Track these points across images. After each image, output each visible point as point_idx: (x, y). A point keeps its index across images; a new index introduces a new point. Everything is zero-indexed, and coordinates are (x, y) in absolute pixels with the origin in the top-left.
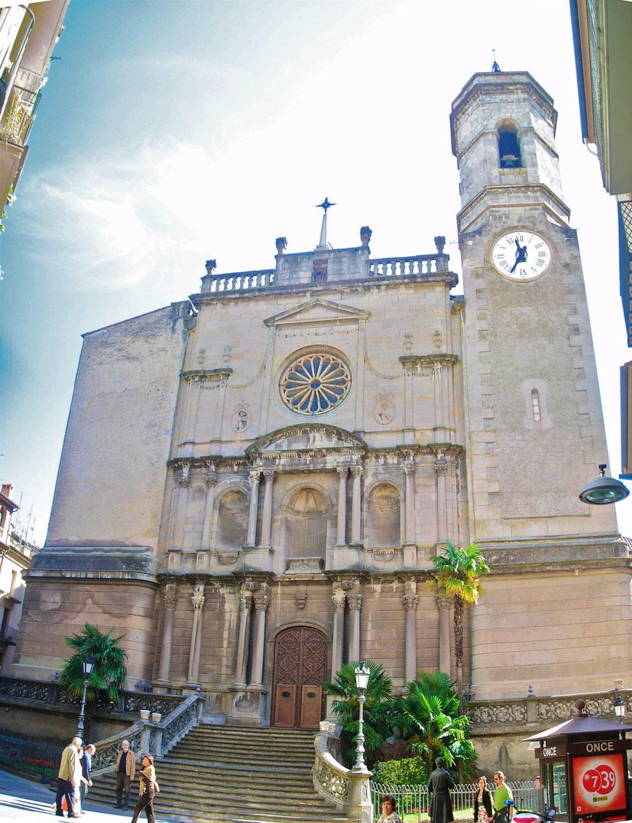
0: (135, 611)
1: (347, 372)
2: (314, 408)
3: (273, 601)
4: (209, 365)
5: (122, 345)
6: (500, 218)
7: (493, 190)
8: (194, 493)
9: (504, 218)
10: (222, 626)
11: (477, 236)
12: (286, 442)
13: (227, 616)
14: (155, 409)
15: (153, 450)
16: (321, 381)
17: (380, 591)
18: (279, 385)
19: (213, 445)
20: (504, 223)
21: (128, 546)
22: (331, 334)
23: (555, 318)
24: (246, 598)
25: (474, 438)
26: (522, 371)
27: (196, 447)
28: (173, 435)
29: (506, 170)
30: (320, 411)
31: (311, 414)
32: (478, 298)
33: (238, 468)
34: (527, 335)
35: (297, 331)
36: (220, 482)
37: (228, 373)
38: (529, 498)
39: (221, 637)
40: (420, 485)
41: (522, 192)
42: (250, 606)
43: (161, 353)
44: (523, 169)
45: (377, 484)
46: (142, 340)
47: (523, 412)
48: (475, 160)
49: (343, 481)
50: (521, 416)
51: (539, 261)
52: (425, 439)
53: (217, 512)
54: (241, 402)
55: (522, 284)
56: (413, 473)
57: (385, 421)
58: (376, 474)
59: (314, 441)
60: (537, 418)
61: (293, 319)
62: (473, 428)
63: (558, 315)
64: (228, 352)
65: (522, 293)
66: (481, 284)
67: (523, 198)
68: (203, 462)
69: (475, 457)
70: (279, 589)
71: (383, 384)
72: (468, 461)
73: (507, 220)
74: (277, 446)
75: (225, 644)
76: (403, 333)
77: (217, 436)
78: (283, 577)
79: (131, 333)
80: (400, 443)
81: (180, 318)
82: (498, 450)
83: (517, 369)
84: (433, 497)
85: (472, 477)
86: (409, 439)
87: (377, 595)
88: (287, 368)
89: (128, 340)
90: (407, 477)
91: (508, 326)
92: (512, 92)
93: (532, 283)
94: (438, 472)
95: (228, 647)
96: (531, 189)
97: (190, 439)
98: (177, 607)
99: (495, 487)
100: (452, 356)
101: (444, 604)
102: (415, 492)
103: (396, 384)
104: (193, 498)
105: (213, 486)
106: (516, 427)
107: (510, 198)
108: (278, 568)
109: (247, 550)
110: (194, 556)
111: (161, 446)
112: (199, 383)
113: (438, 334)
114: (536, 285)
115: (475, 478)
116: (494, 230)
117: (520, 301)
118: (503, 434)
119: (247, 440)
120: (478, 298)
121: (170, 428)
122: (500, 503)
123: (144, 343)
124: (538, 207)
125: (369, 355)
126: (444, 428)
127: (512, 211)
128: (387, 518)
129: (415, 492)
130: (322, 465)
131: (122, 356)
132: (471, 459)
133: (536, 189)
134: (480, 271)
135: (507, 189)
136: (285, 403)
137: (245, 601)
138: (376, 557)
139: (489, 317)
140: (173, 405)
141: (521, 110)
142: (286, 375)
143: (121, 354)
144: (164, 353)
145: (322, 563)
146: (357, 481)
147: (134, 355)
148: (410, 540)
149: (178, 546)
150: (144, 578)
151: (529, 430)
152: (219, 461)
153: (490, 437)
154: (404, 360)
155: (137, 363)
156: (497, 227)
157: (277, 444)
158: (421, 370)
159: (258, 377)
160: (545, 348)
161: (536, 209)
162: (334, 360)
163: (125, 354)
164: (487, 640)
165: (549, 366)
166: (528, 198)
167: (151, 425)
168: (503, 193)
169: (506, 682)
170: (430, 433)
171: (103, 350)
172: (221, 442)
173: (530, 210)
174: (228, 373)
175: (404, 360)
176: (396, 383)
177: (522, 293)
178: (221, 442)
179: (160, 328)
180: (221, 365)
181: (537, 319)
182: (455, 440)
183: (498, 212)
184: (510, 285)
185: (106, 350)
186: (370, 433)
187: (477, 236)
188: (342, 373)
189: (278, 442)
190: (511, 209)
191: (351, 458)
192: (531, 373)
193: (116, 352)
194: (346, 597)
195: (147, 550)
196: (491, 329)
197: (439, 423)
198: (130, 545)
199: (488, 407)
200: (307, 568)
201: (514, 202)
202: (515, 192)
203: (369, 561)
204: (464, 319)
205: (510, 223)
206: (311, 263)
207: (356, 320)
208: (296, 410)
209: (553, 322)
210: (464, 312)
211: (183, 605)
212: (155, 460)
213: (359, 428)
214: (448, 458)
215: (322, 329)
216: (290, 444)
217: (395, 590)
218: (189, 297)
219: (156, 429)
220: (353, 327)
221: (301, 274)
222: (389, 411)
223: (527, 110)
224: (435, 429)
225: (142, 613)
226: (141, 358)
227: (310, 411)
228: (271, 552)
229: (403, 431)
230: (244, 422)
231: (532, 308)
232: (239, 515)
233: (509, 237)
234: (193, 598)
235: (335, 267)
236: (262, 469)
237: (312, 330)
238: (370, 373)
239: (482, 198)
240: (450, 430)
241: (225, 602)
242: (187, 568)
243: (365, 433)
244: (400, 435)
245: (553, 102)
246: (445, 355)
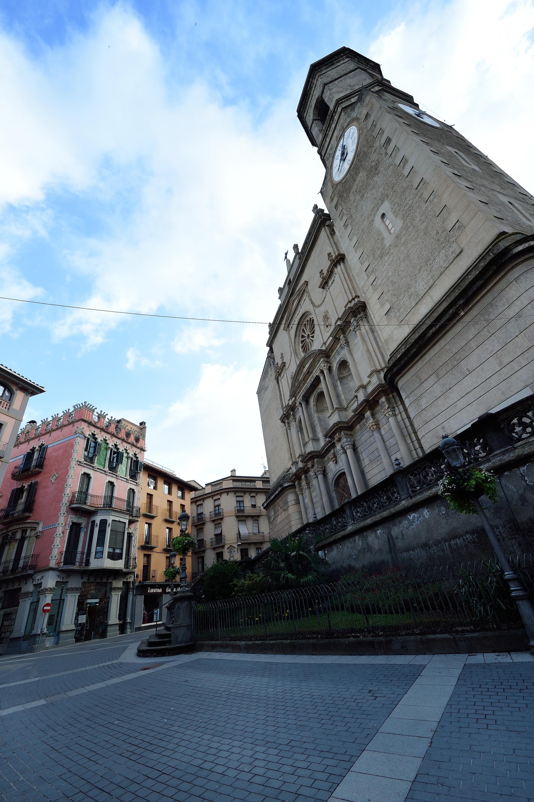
0: (290, 504)
38: (410, 290)
99: (387, 306)
125: (313, 301)
150: (286, 485)
151: (390, 246)
164: (419, 425)
202: (330, 129)
207: (304, 290)
225: (293, 502)
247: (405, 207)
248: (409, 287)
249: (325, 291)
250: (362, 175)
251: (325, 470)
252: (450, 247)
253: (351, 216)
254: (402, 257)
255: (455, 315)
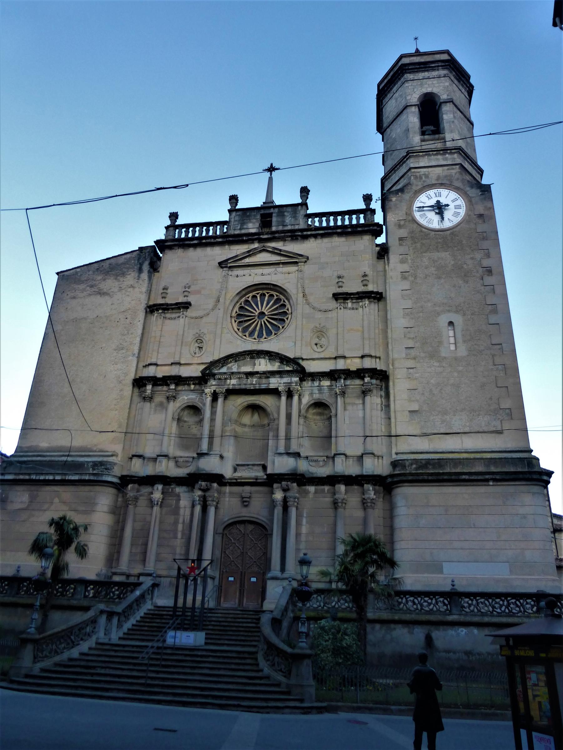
0: (99, 508)
1: (288, 306)
2: (260, 335)
3: (222, 499)
4: (170, 300)
5: (94, 282)
6: (421, 178)
7: (415, 154)
8: (156, 407)
9: (423, 178)
10: (176, 523)
11: (400, 194)
12: (236, 366)
13: (182, 511)
14: (123, 335)
15: (121, 370)
16: (266, 313)
17: (314, 492)
18: (231, 317)
19: (174, 366)
20: (424, 181)
21: (95, 451)
22: (275, 274)
23: (470, 262)
24: (199, 496)
25: (397, 365)
26: (440, 306)
27: (159, 368)
28: (138, 357)
29: (426, 137)
30: (265, 338)
31: (258, 340)
32: (400, 245)
33: (195, 387)
34: (443, 276)
35: (247, 271)
36: (179, 398)
37: (186, 306)
38: (445, 416)
39: (175, 532)
40: (349, 404)
41: (441, 154)
42: (202, 503)
43: (129, 290)
44: (441, 136)
45: (312, 402)
46: (112, 278)
47: (440, 343)
48: (399, 130)
49: (284, 398)
50: (438, 346)
51: (455, 212)
52: (354, 365)
53: (175, 424)
54: (199, 332)
55: (439, 232)
56: (343, 393)
57: (320, 350)
58: (311, 394)
59: (260, 365)
60: (452, 347)
61: (243, 261)
62: (396, 356)
63: (472, 258)
64: (186, 291)
65: (439, 240)
66: (403, 233)
67: (441, 160)
68: (165, 381)
69: (396, 381)
70: (227, 489)
71: (319, 315)
72: (391, 384)
73: (427, 179)
74: (228, 368)
75: (179, 535)
76: (336, 274)
77: (177, 360)
78: (231, 479)
79: (102, 272)
80: (333, 368)
81: (146, 260)
82: (417, 375)
83: (435, 304)
84: (361, 414)
85: (394, 397)
86: (341, 365)
87: (311, 496)
88: (237, 302)
89: (99, 278)
90: (338, 396)
91: (426, 268)
92: (433, 69)
93: (449, 232)
94: (365, 393)
95: (182, 538)
96: (449, 151)
97: (154, 361)
98: (138, 504)
99: (415, 407)
100: (377, 293)
101: (369, 504)
102: (345, 409)
103: (330, 316)
104: (155, 410)
105: (172, 401)
106: (434, 355)
107: (430, 160)
108: (228, 473)
109: (201, 455)
110: (155, 460)
111: (127, 366)
112: (163, 315)
113: (365, 275)
114: (452, 233)
115: (397, 398)
116: (415, 188)
117: (437, 247)
118: (422, 361)
119: (202, 363)
120: (400, 245)
121: (136, 351)
122: (419, 420)
123: (114, 281)
124: (454, 167)
125: (306, 292)
126: (370, 356)
127: (431, 171)
128: (320, 432)
129: (345, 409)
130: (266, 385)
131: (94, 291)
132: (394, 382)
133: (453, 151)
134: (402, 223)
135: (427, 153)
136: (235, 332)
137: (198, 499)
138: (311, 463)
139: (410, 261)
140: (140, 332)
141: (442, 84)
142: (236, 309)
143: (93, 289)
144: (132, 289)
145: (264, 468)
146: (296, 398)
147: (105, 290)
148: (341, 449)
149: (140, 452)
150: (109, 479)
151: (445, 358)
152: (179, 380)
153: (410, 363)
154: (336, 297)
155: (107, 297)
156: (417, 185)
157: (229, 367)
158: (352, 305)
159: (213, 309)
160: (460, 287)
161: (453, 169)
162: (277, 296)
163: (97, 290)
165: (464, 302)
166: (446, 159)
167: (119, 348)
168: (423, 156)
169: (426, 575)
170: (358, 361)
171: (76, 286)
172: (179, 364)
173: (448, 169)
174: (186, 306)
175: (336, 297)
176: (330, 315)
177: (439, 240)
178: (179, 364)
179: (128, 268)
180: (181, 299)
181: (452, 262)
182: (379, 366)
183: (419, 172)
184: (429, 234)
185: (79, 286)
186: (307, 359)
187: (400, 194)
188: (284, 306)
189: (230, 365)
190: (430, 169)
191: (291, 380)
192: (447, 308)
193: (88, 288)
194: (285, 497)
195: (112, 456)
196: (412, 271)
197: (367, 352)
198: (97, 450)
199: (409, 338)
200: (251, 471)
201: (434, 163)
203: (303, 466)
204: (388, 263)
205: (429, 182)
206: (259, 217)
207: (296, 263)
208: (245, 337)
209: (468, 265)
210: (388, 256)
211: (142, 502)
212: (121, 379)
213: (298, 355)
214: (374, 381)
215: (267, 270)
216: (239, 367)
217: (326, 492)
218: (155, 242)
219: (124, 351)
220: (293, 268)
221: (250, 225)
222: (323, 341)
223: (447, 84)
224: (362, 357)
225: (106, 509)
226: (111, 294)
227: (256, 338)
228: (222, 457)
229: (335, 358)
230: (200, 348)
231: (448, 253)
232: (194, 426)
233: (428, 194)
234: (152, 496)
235: (279, 220)
236: (213, 388)
237: (259, 271)
238: (307, 306)
239: (405, 162)
240: (376, 357)
241: (180, 500)
242: (149, 470)
243: (303, 359)
244: (333, 361)
245: (469, 78)
246: (372, 292)
247: (475, 344)
248: (445, 413)
249: (333, 304)
250: (445, 257)
251: (218, 501)
252: (495, 420)
253: (415, 277)
254: (452, 381)
255: (487, 480)
